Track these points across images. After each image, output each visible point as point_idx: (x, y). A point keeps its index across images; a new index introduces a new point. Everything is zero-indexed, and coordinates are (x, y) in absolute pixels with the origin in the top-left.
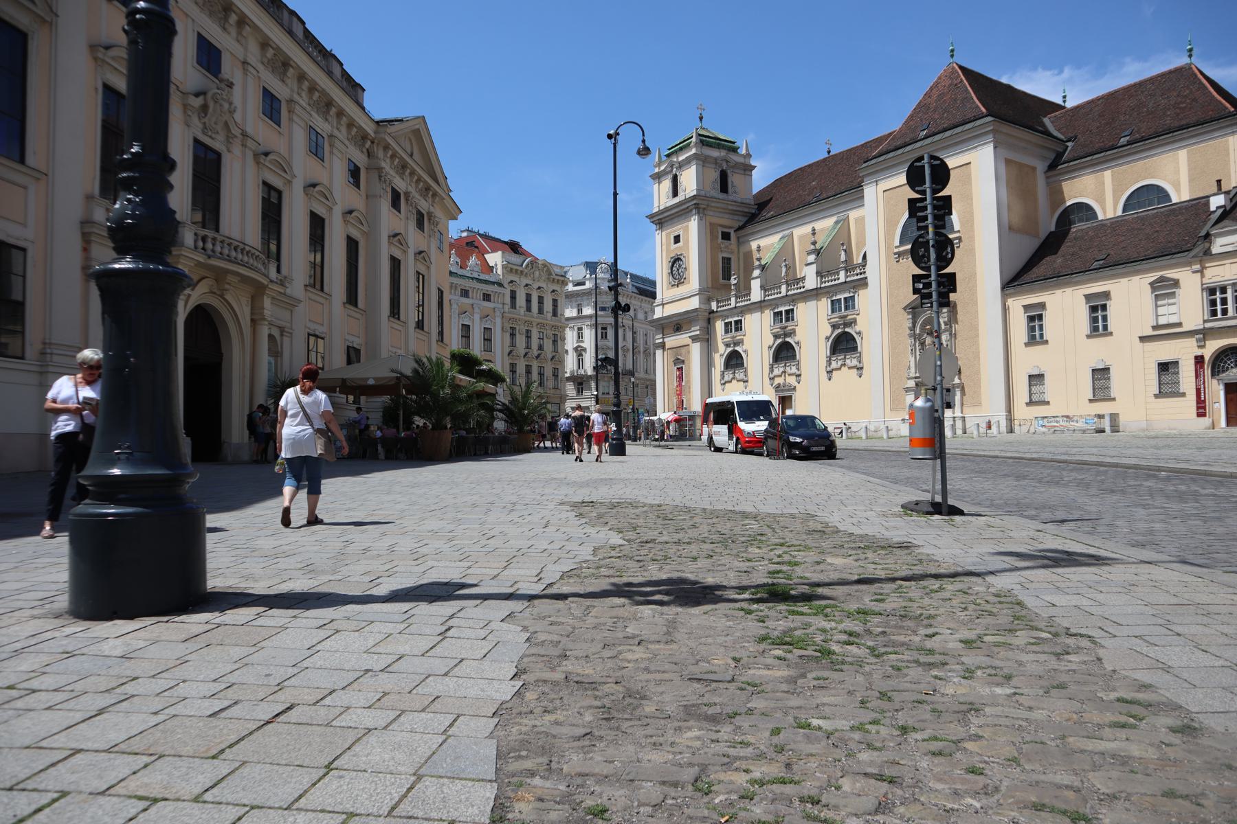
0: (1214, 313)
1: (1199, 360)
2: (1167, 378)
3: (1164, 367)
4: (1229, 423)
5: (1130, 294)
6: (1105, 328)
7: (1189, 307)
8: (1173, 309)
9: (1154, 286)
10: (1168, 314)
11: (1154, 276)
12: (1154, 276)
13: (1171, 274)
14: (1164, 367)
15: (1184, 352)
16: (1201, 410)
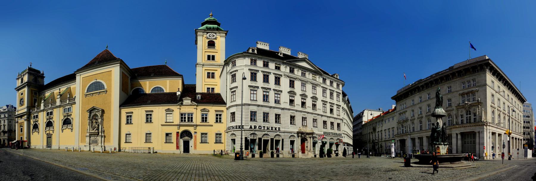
0: (182, 121)
1: (178, 133)
2: (168, 138)
3: (167, 135)
4: (184, 152)
5: (159, 111)
6: (151, 121)
7: (175, 118)
8: (171, 118)
9: (166, 110)
10: (170, 119)
11: (167, 108)
12: (167, 108)
13: (172, 107)
14: (167, 135)
15: (174, 130)
16: (178, 147)
